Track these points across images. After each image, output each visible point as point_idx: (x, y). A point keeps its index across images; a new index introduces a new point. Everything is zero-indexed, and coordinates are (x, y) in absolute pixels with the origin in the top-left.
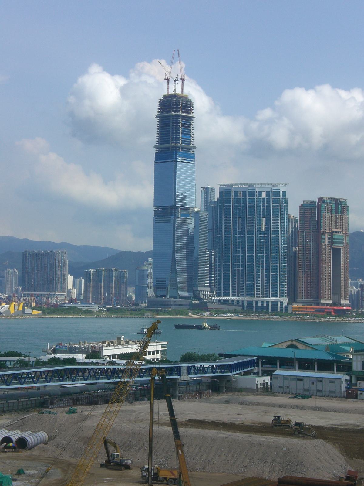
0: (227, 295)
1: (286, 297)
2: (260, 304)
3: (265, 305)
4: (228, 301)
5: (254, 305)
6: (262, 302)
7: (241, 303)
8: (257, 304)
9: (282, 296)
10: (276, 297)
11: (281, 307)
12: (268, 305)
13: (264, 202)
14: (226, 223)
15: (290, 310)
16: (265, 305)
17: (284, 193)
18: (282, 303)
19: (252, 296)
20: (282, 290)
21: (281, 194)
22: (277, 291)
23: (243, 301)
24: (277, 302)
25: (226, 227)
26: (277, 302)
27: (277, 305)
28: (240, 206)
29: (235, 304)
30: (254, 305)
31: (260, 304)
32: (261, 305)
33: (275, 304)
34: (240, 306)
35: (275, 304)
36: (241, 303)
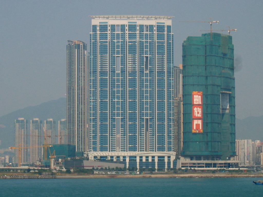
0: (102, 149)
1: (173, 151)
2: (144, 160)
3: (150, 160)
4: (106, 157)
5: (138, 160)
6: (147, 157)
7: (121, 159)
8: (141, 160)
9: (169, 149)
10: (162, 151)
11: (169, 163)
12: (153, 160)
13: (146, 38)
14: (102, 61)
15: (179, 166)
16: (150, 160)
17: (169, 27)
18: (169, 157)
19: (135, 151)
20: (169, 143)
21: (166, 29)
22: (164, 143)
23: (124, 157)
24: (164, 157)
25: (102, 68)
26: (164, 157)
27: (164, 160)
28: (118, 42)
29: (115, 160)
30: (138, 160)
31: (144, 160)
32: (146, 160)
33: (161, 159)
34: (121, 163)
35: (161, 159)
36: (121, 159)
